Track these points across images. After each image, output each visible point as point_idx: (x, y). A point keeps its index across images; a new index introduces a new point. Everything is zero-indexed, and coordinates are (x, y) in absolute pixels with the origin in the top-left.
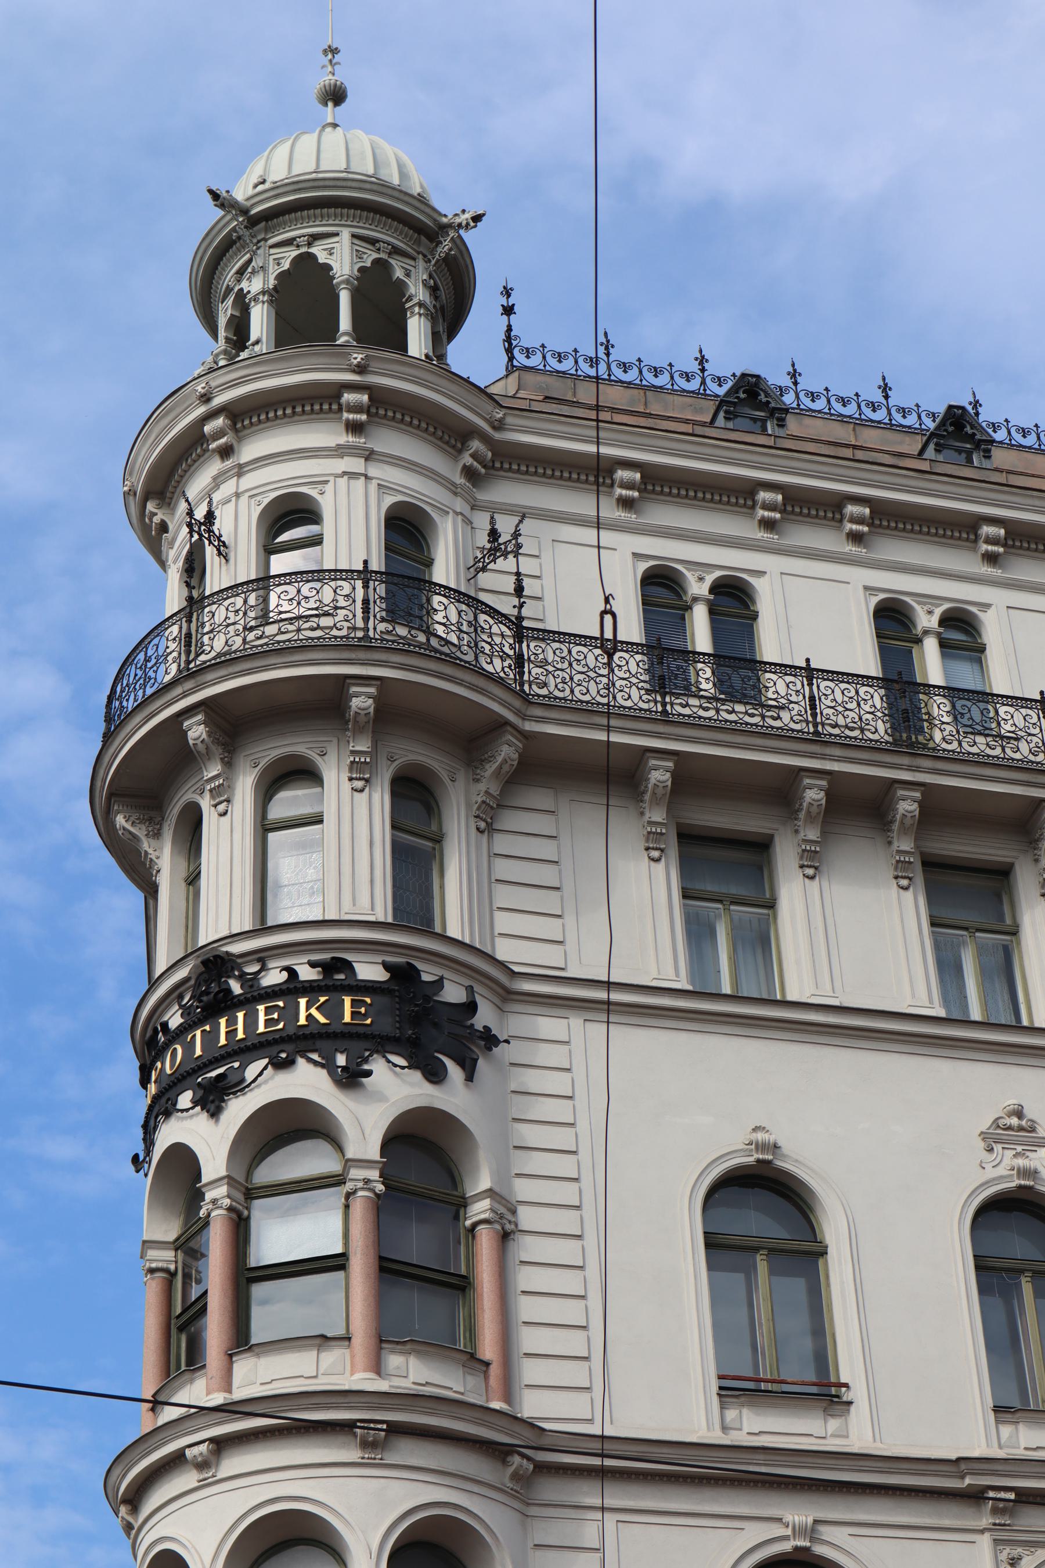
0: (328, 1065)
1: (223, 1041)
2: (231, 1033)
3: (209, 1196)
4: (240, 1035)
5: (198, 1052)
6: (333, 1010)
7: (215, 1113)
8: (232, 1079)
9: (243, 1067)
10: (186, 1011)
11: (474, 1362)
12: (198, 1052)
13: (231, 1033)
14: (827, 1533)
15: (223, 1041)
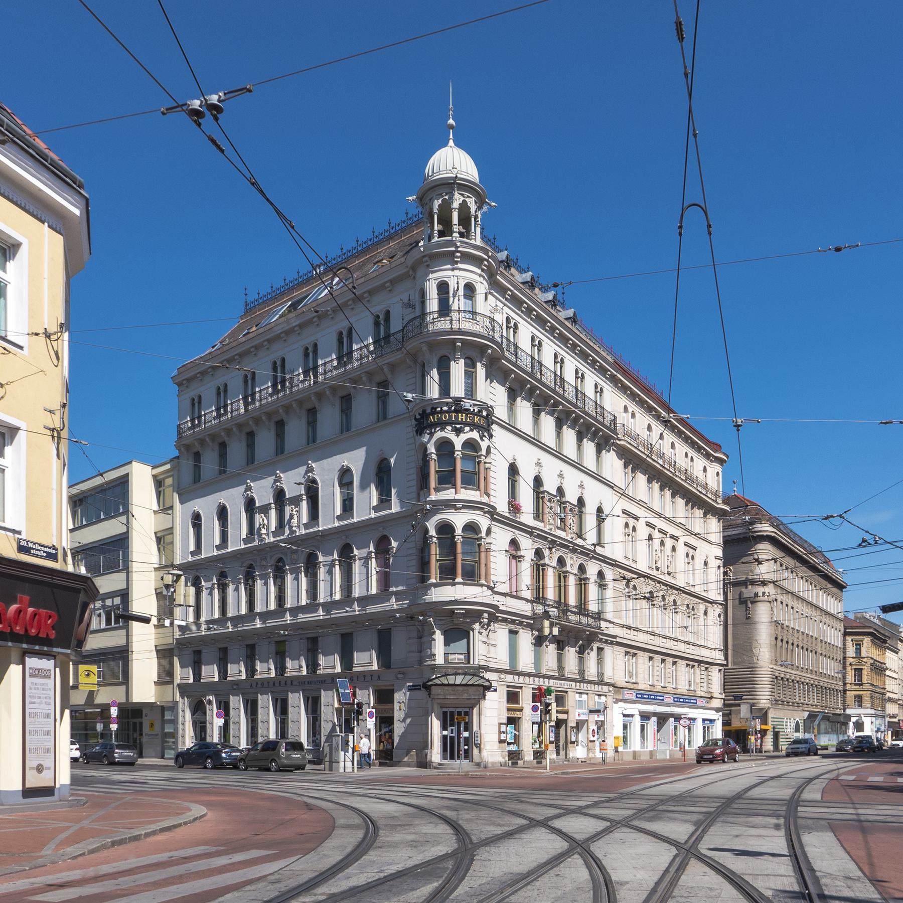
0: (479, 433)
1: (460, 420)
2: (462, 419)
3: (456, 453)
4: (464, 420)
5: (453, 419)
6: (480, 420)
7: (458, 436)
8: (462, 429)
9: (464, 427)
10: (450, 408)
11: (488, 495)
12: (453, 419)
13: (462, 419)
14: (518, 535)
15: (460, 420)
